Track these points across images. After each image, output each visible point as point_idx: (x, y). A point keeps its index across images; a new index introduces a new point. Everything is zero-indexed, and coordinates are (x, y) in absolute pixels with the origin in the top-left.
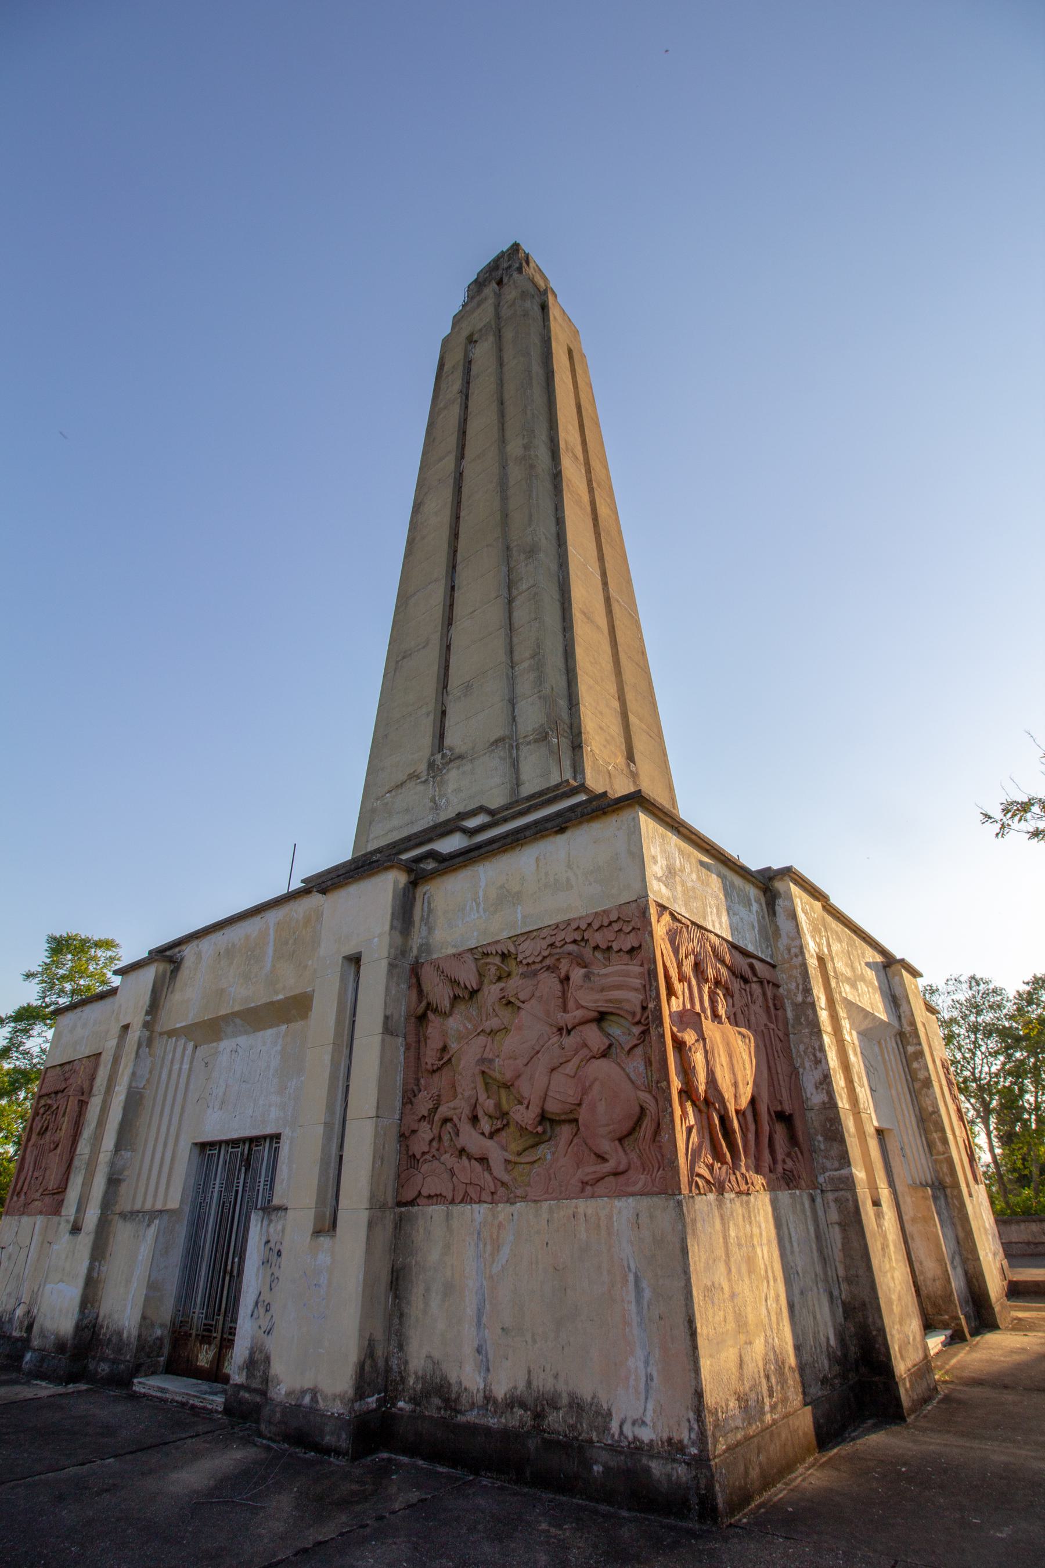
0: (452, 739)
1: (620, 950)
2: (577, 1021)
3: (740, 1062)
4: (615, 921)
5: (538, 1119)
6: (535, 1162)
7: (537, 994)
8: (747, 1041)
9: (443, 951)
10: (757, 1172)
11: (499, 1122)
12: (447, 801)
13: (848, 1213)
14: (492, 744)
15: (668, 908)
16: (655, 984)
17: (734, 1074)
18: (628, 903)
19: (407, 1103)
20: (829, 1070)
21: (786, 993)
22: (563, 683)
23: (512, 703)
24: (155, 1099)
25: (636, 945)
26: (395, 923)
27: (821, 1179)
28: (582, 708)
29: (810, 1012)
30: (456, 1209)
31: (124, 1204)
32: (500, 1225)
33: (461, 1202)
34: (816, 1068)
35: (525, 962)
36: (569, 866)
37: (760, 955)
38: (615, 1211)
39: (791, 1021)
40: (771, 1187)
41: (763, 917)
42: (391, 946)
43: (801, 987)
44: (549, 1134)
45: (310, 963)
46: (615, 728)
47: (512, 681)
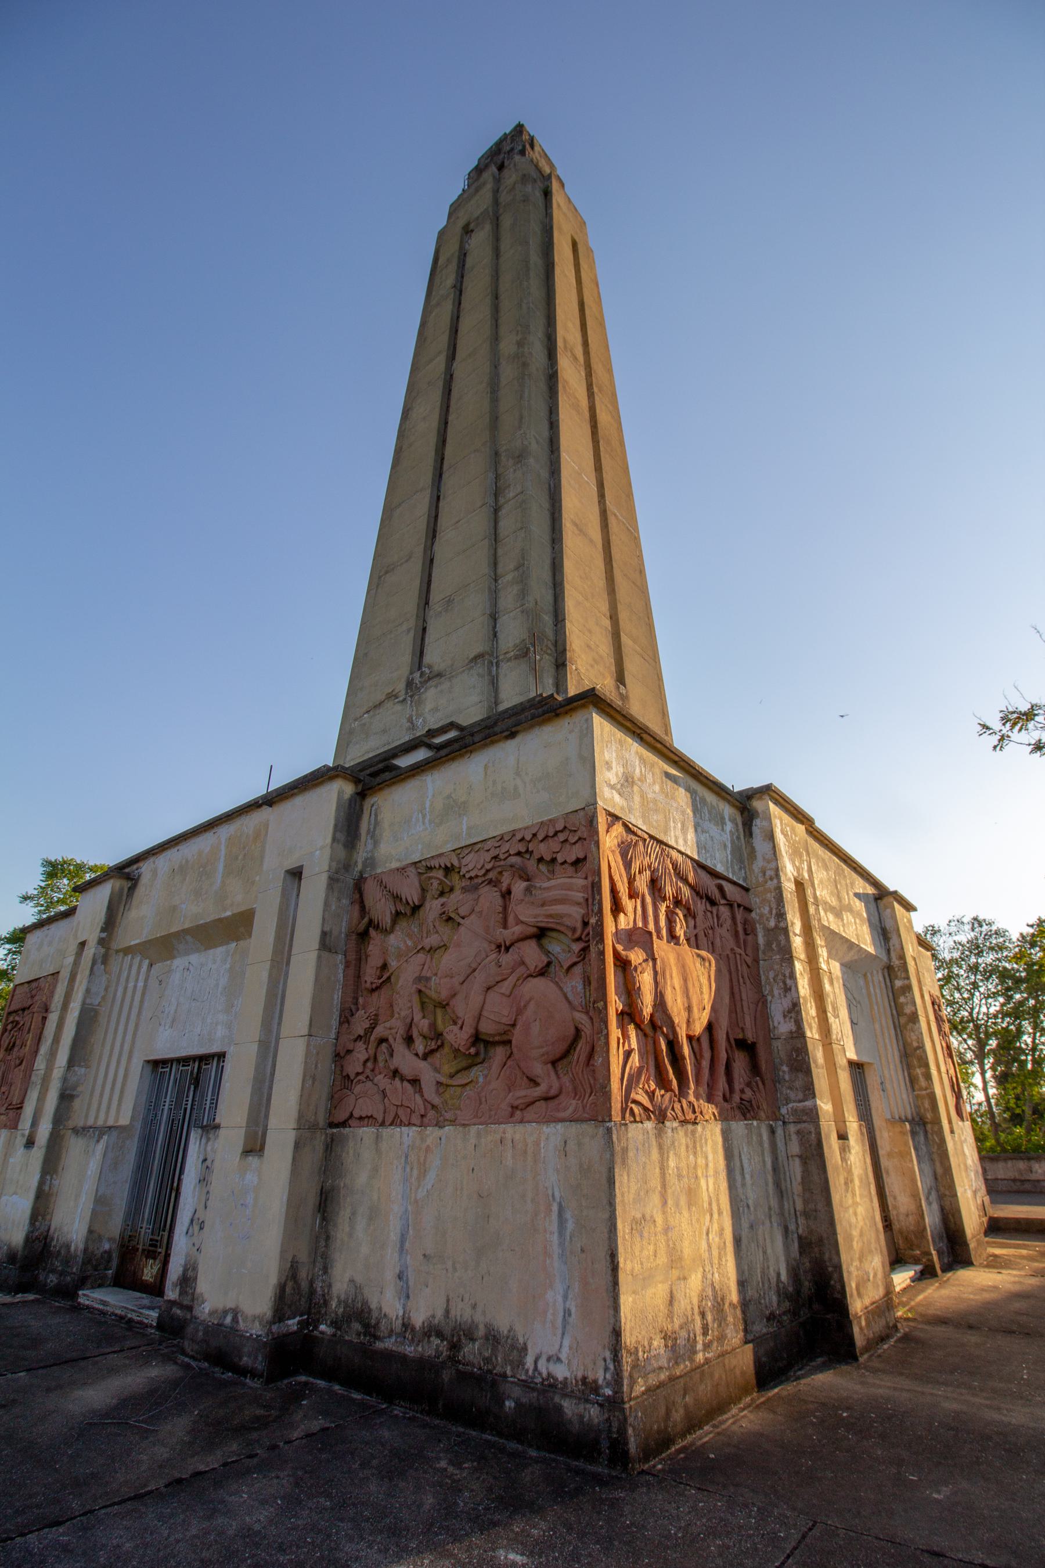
0: (433, 657)
1: (565, 862)
2: (515, 937)
3: (697, 984)
4: (561, 831)
5: (471, 1040)
6: (466, 1084)
7: (477, 909)
8: (707, 964)
9: (387, 865)
10: (710, 1099)
11: (433, 1043)
13: (810, 1146)
14: (471, 661)
15: (621, 818)
16: (597, 897)
17: (688, 997)
18: (576, 811)
19: (344, 1022)
20: (799, 998)
21: (758, 918)
22: (549, 598)
23: (494, 617)
24: (109, 1016)
25: (581, 856)
26: (338, 835)
27: (784, 1111)
28: (568, 625)
29: (782, 938)
30: (386, 1132)
31: (78, 1119)
32: (428, 1149)
33: (391, 1124)
34: (785, 996)
35: (467, 876)
36: (518, 774)
37: (731, 876)
38: (543, 1138)
39: (762, 947)
40: (724, 1117)
41: (738, 838)
42: (332, 859)
43: (774, 912)
44: (482, 1056)
45: (257, 878)
46: (605, 649)
47: (494, 595)
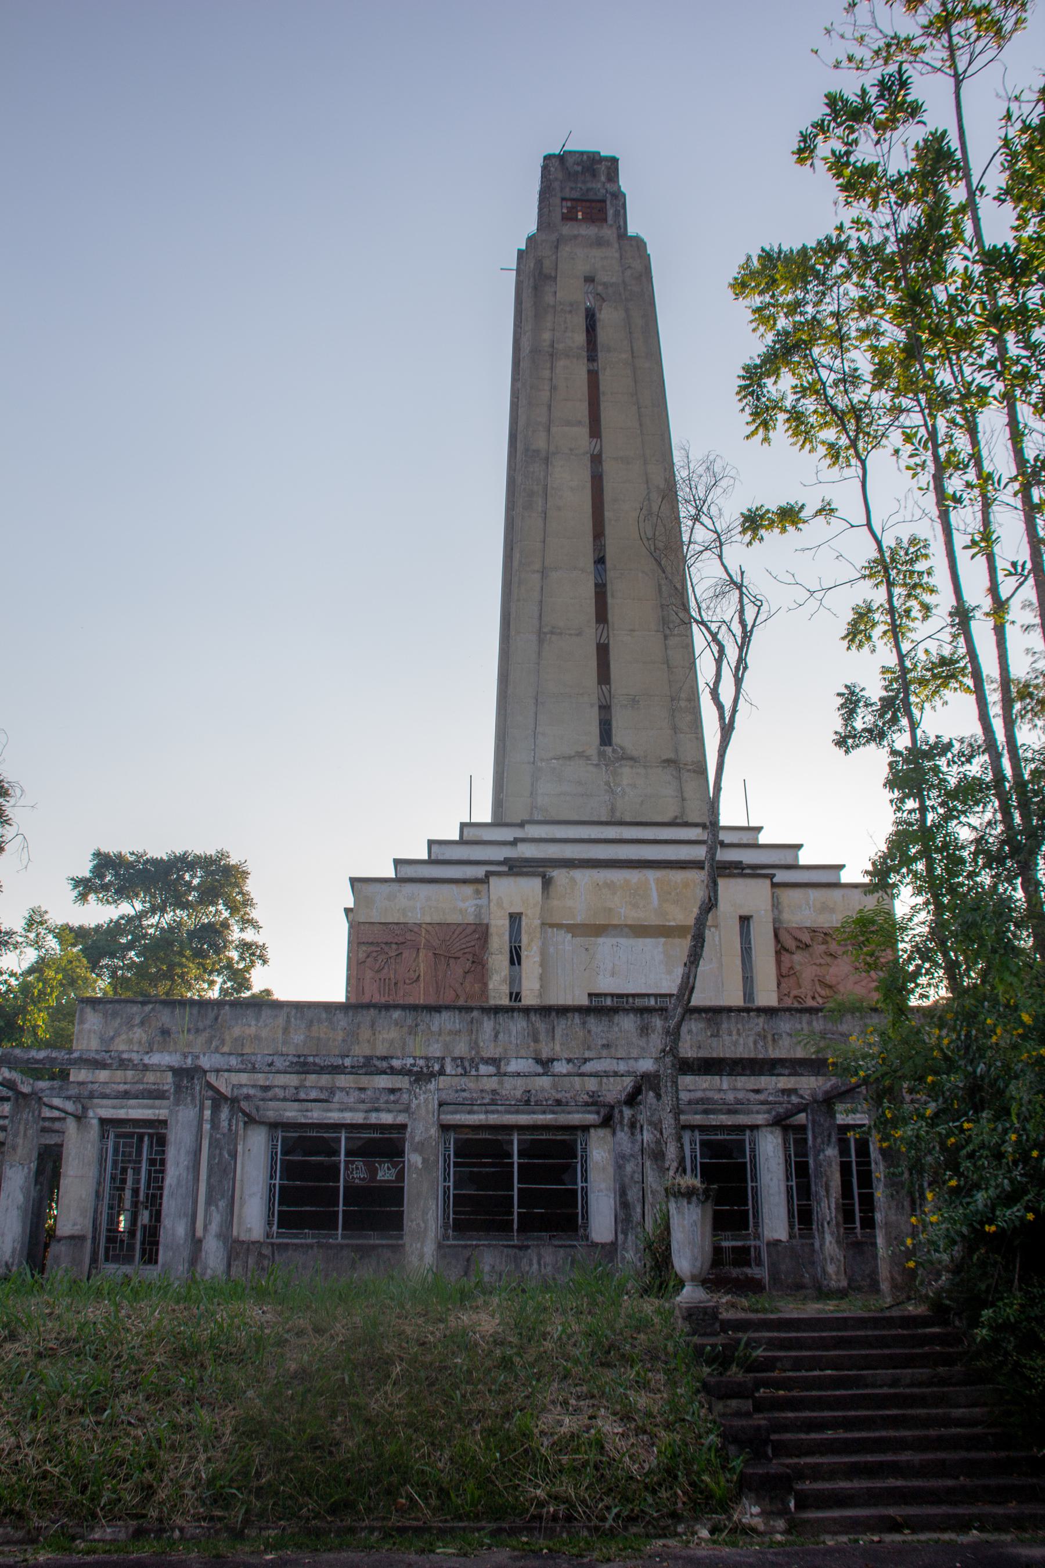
12: (623, 790)
